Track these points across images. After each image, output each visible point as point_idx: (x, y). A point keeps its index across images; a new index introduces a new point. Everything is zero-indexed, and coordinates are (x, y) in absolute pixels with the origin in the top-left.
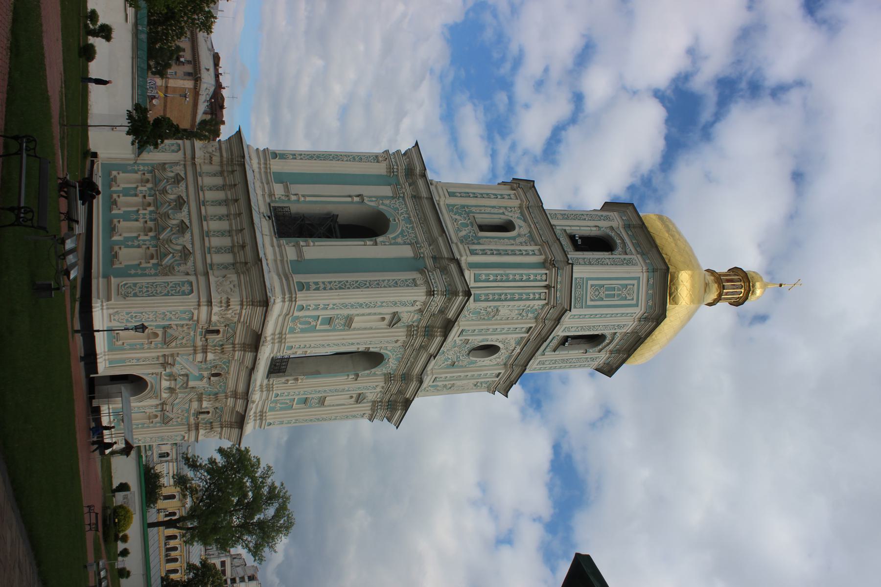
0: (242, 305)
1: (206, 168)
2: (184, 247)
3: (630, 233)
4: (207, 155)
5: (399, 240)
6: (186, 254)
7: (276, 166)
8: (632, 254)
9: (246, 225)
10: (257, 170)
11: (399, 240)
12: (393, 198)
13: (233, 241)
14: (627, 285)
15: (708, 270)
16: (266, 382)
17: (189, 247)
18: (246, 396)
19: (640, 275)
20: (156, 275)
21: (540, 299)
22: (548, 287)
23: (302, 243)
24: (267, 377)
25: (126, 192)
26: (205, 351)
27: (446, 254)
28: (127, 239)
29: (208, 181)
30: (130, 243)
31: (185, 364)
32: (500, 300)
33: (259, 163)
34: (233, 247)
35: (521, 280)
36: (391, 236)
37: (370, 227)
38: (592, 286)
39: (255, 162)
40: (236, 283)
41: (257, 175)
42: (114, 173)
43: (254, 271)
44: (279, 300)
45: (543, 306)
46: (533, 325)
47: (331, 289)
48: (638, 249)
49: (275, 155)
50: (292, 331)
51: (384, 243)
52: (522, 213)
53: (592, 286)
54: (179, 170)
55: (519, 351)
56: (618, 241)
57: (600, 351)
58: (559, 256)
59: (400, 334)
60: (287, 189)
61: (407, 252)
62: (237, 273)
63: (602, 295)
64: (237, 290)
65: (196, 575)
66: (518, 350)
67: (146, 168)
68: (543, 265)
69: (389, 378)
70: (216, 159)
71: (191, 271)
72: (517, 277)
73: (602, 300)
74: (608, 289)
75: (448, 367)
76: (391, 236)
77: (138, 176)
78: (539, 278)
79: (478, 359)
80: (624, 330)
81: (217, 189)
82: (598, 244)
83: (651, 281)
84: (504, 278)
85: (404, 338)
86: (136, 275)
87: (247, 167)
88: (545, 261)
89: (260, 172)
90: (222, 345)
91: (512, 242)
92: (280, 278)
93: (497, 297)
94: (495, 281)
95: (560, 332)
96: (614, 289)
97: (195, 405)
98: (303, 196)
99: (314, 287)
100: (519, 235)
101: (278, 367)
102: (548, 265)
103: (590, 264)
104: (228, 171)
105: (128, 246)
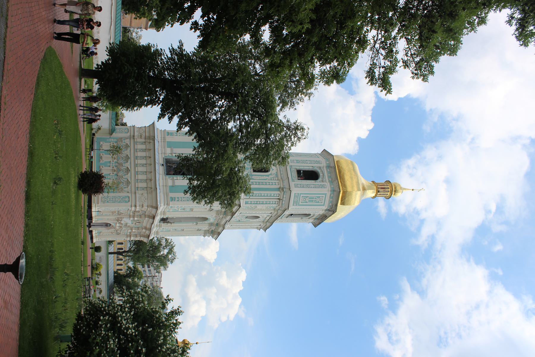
1: (139, 140)
3: (328, 170)
9: (153, 170)
10: (160, 141)
18: (150, 229)
19: (327, 193)
21: (275, 204)
23: (175, 178)
26: (134, 217)
29: (140, 147)
31: (125, 220)
32: (257, 204)
42: (101, 143)
43: (154, 193)
44: (162, 205)
54: (127, 141)
56: (321, 175)
58: (287, 186)
60: (172, 150)
65: (130, 272)
70: (143, 136)
71: (130, 192)
72: (266, 195)
74: (310, 198)
81: (143, 151)
82: (311, 175)
83: (332, 195)
88: (280, 187)
91: (267, 177)
95: (287, 213)
100: (271, 174)
103: (303, 187)
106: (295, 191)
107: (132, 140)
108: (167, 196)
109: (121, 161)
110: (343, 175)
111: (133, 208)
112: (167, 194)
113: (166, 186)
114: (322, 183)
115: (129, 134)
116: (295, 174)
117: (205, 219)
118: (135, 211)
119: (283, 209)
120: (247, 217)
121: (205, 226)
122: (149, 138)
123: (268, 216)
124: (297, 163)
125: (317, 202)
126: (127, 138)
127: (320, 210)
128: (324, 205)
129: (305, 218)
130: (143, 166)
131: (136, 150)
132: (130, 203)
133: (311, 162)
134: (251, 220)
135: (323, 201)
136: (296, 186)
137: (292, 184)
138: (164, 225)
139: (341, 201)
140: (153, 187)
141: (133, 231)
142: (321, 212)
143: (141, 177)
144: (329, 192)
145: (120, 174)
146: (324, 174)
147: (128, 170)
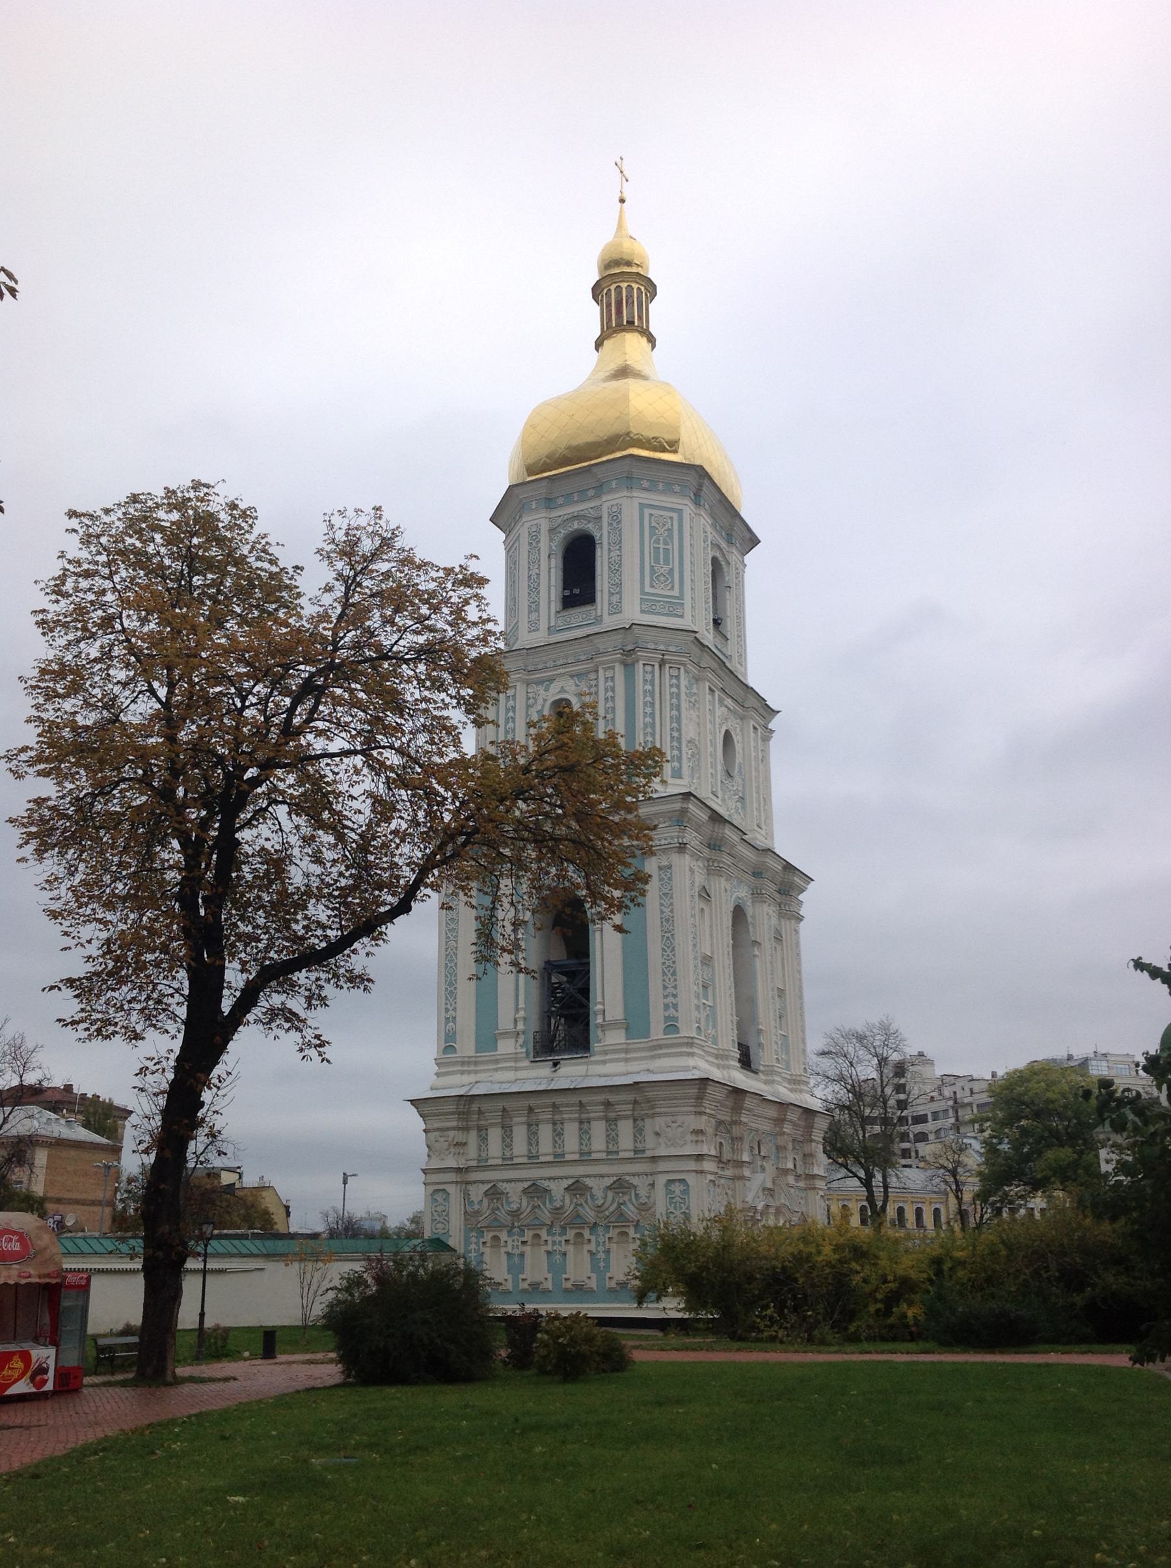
0: (701, 1113)
2: (609, 1188)
4: (452, 1150)
6: (620, 1186)
7: (466, 1047)
8: (599, 508)
9: (574, 1099)
10: (472, 1078)
13: (599, 1119)
15: (597, 349)
16: (761, 1076)
17: (608, 1181)
18: (783, 1106)
19: (636, 502)
21: (678, 677)
23: (599, 1020)
24: (755, 1072)
26: (740, 1164)
28: (595, 1267)
30: (602, 1264)
32: (679, 739)
33: (462, 1073)
34: (607, 1120)
35: (652, 704)
38: (652, 586)
40: (669, 1119)
41: (479, 1077)
44: (691, 1062)
45: (686, 671)
46: (707, 684)
47: (675, 987)
48: (591, 493)
49: (449, 1048)
50: (715, 1042)
52: (539, 682)
53: (652, 586)
54: (477, 1192)
55: (729, 700)
56: (576, 525)
57: (728, 563)
58: (617, 640)
59: (719, 886)
60: (505, 1034)
62: (653, 1116)
63: (667, 568)
64: (680, 1119)
66: (729, 702)
67: (474, 1240)
68: (629, 666)
69: (757, 895)
70: (460, 1136)
71: (650, 1179)
73: (672, 570)
74: (657, 561)
75: (743, 808)
78: (649, 677)
79: (737, 761)
80: (709, 529)
81: (510, 1137)
83: (646, 484)
84: (649, 730)
85: (722, 879)
87: (474, 1092)
89: (476, 1072)
90: (732, 1139)
92: (660, 1056)
93: (675, 744)
95: (709, 637)
98: (517, 1010)
101: (746, 1061)
102: (629, 660)
104: (479, 1119)
105: (607, 1267)
106: (632, 612)
107: (473, 1176)
108: (660, 1047)
109: (546, 1216)
110: (578, 448)
111: (709, 1166)
112: (655, 1048)
114: (605, 520)
115: (451, 1189)
116: (578, 614)
117: (739, 913)
118: (719, 1159)
119: (696, 650)
120: (729, 775)
121: (764, 917)
122: (463, 1115)
123: (721, 701)
124: (537, 610)
125: (671, 536)
126: (467, 1195)
127: (697, 528)
128: (680, 512)
129: (729, 577)
130: (560, 1134)
131: (508, 1163)
132: (691, 1179)
133: (534, 562)
134: (739, 759)
135: (671, 514)
136: (616, 609)
137: (609, 622)
138: (765, 1057)
139: (664, 450)
141: (790, 1165)
142: (705, 521)
143: (598, 1142)
144: (635, 494)
145: (589, 1214)
146: (572, 514)
147: (577, 1188)
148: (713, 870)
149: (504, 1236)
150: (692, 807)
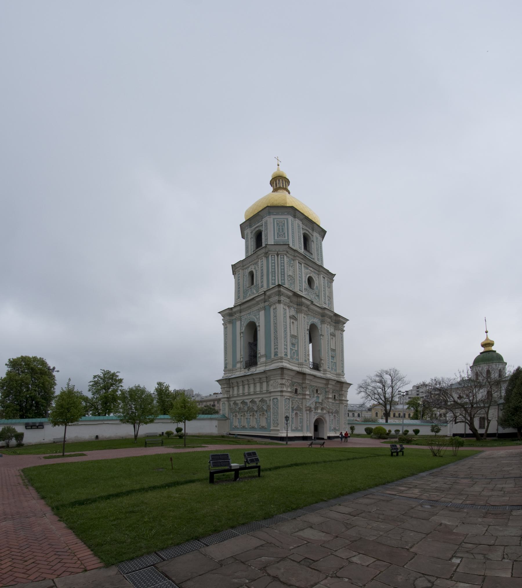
0: (283, 379)
1: (231, 393)
2: (260, 401)
5: (258, 317)
6: (262, 401)
7: (230, 367)
11: (258, 317)
12: (241, 321)
14: (277, 223)
17: (260, 399)
20: (270, 412)
21: (283, 258)
22: (278, 255)
25: (240, 422)
27: (263, 297)
29: (236, 392)
32: (284, 274)
35: (275, 266)
36: (256, 320)
37: (253, 328)
39: (227, 375)
42: (233, 427)
43: (269, 374)
51: (259, 323)
54: (232, 403)
60: (238, 362)
61: (262, 313)
63: (282, 234)
72: (273, 267)
73: (284, 233)
76: (256, 320)
77: (234, 418)
78: (273, 259)
86: (270, 419)
94: (275, 276)
96: (279, 229)
97: (330, 400)
99: (276, 350)
105: (259, 423)
109: (246, 408)
113: (266, 363)
132: (279, 398)
140: (264, 376)
145: (255, 408)
148: (298, 311)
149: (237, 414)
150: (282, 289)
